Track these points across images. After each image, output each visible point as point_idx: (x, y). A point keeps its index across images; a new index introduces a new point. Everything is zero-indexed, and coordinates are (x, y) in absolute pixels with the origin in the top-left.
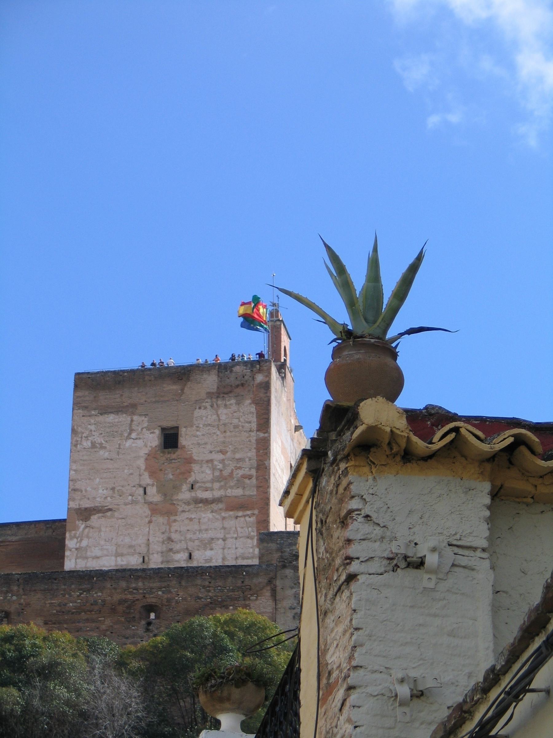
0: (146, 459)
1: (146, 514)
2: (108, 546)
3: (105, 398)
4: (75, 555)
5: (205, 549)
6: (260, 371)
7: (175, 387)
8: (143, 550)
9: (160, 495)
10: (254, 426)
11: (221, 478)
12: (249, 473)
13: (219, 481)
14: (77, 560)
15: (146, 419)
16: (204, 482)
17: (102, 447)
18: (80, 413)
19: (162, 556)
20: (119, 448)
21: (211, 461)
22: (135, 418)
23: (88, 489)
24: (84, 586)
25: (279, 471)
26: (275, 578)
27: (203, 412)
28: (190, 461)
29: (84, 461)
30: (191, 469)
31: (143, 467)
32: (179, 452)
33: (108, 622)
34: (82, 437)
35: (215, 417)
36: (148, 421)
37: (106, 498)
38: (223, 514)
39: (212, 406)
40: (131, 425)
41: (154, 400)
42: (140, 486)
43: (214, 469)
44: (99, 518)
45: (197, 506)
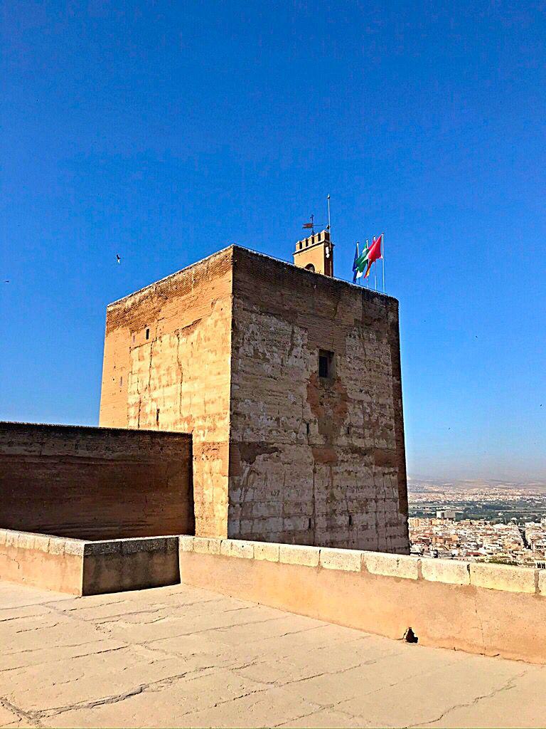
0: (308, 386)
1: (310, 461)
2: (275, 501)
4: (239, 513)
8: (308, 509)
9: (322, 436)
14: (242, 522)
15: (306, 334)
18: (241, 304)
19: (327, 520)
21: (361, 402)
23: (251, 415)
28: (345, 398)
29: (246, 373)
30: (347, 409)
34: (243, 339)
35: (362, 349)
37: (271, 431)
41: (312, 312)
43: (364, 413)
45: (354, 456)
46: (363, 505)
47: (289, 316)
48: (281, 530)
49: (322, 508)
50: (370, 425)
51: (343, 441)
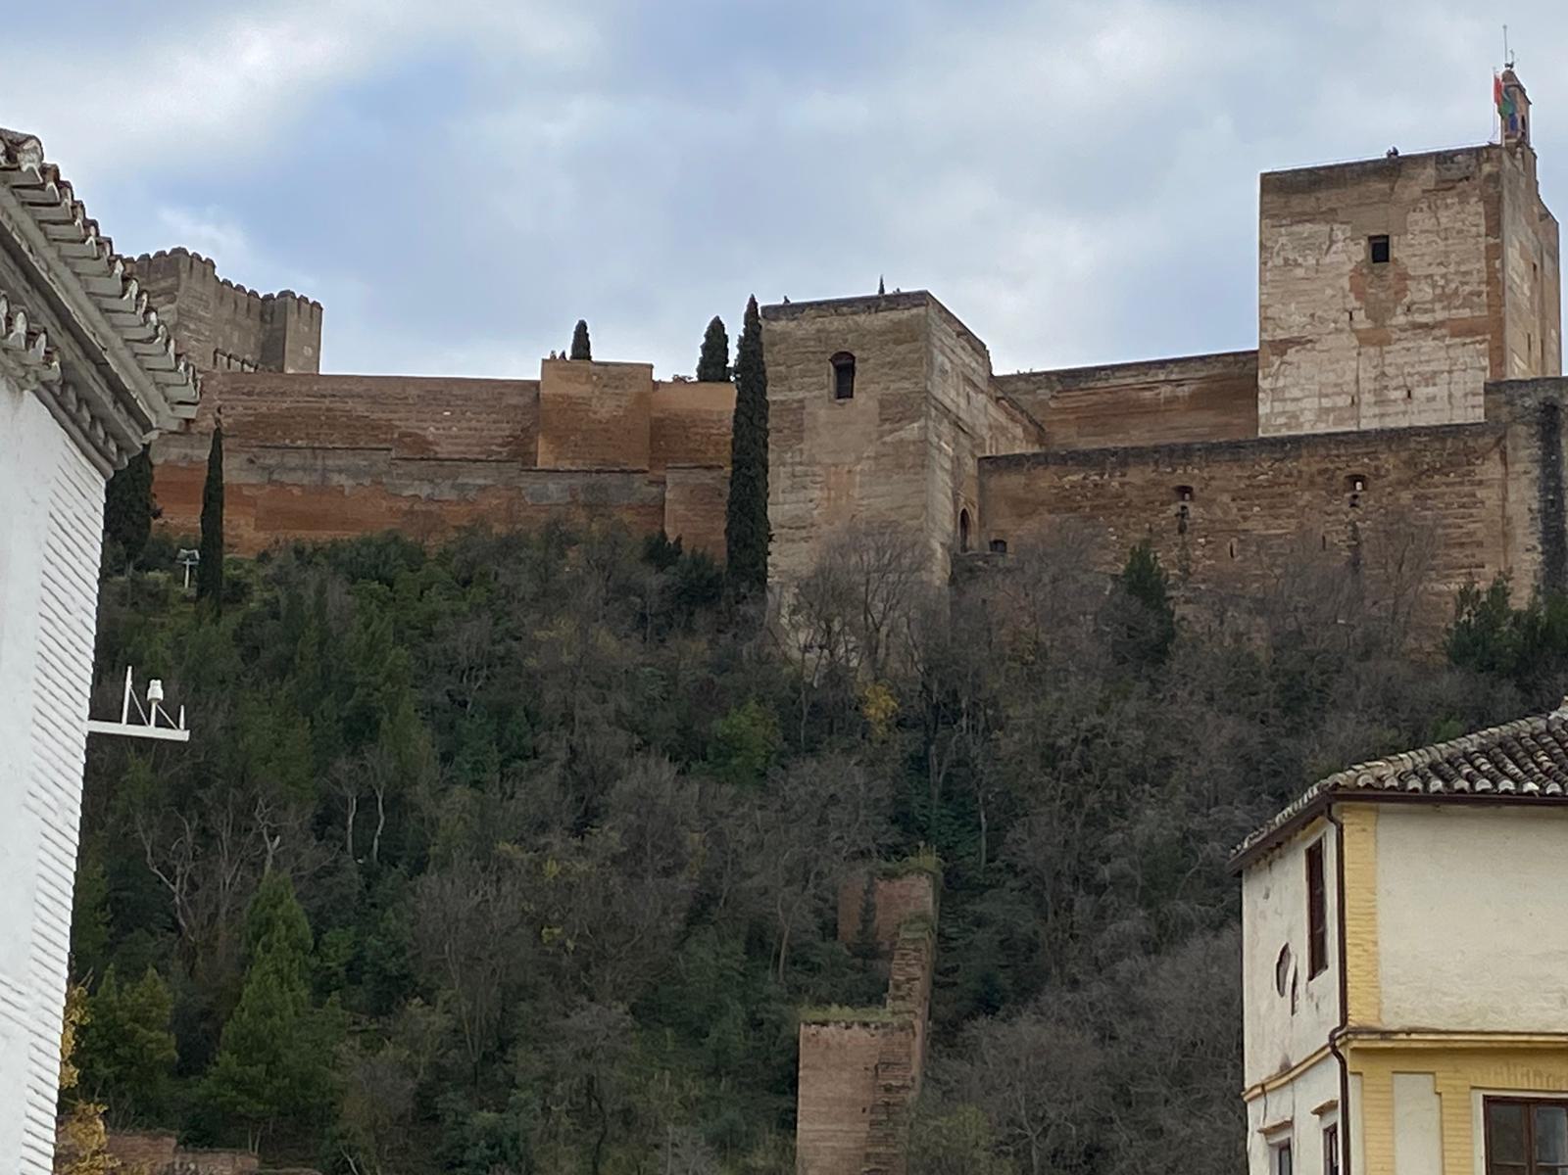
3: (1298, 203)
5: (1427, 386)
6: (1488, 160)
7: (1385, 186)
8: (1354, 389)
10: (1483, 230)
11: (1445, 298)
12: (1477, 289)
13: (1441, 301)
16: (1424, 303)
17: (1300, 265)
20: (1318, 264)
22: (1335, 227)
24: (1277, 456)
25: (1517, 280)
26: (1503, 438)
27: (1417, 216)
28: (1404, 277)
31: (1347, 286)
32: (1390, 266)
33: (1307, 496)
35: (1433, 220)
36: (1352, 230)
38: (1448, 341)
39: (1429, 207)
40: (1330, 236)
43: (1434, 286)
46: (1430, 379)
47: (1330, 216)
49: (1367, 385)
50: (1445, 298)
51: (1401, 320)
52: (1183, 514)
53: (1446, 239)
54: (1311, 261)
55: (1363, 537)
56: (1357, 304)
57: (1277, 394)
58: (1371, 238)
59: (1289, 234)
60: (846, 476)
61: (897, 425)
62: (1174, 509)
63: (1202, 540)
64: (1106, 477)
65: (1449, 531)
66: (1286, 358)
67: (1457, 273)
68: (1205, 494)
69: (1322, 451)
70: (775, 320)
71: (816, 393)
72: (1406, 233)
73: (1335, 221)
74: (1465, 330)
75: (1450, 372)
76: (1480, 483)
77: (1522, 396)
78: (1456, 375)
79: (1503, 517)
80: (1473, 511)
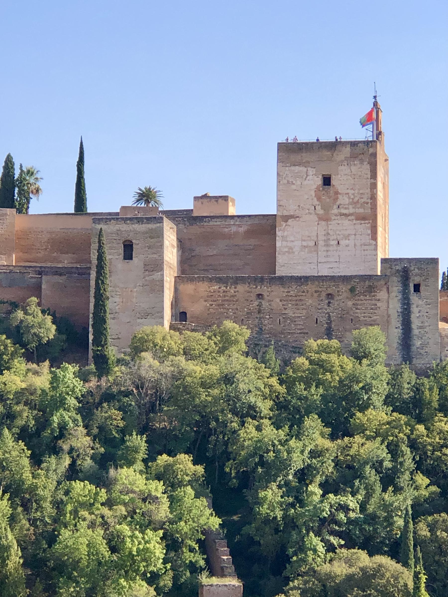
0: (315, 191)
5: (346, 239)
6: (371, 147)
10: (369, 176)
13: (351, 205)
17: (294, 184)
20: (301, 184)
22: (309, 169)
27: (343, 167)
28: (337, 193)
31: (314, 195)
33: (310, 301)
35: (349, 170)
37: (295, 211)
38: (354, 222)
39: (348, 165)
42: (313, 205)
43: (349, 198)
44: (292, 221)
46: (347, 237)
47: (306, 164)
48: (300, 245)
49: (321, 238)
52: (260, 305)
53: (354, 179)
54: (299, 183)
55: (332, 319)
56: (318, 203)
57: (284, 238)
58: (323, 175)
59: (289, 170)
60: (130, 293)
61: (151, 273)
62: (256, 303)
63: (268, 317)
64: (228, 288)
65: (366, 319)
66: (288, 223)
67: (358, 193)
68: (269, 298)
69: (317, 283)
70: (99, 224)
71: (117, 257)
72: (338, 175)
73: (309, 166)
74: (362, 218)
75: (355, 235)
76: (379, 300)
77: (395, 265)
78: (357, 236)
79: (387, 314)
80: (376, 311)
